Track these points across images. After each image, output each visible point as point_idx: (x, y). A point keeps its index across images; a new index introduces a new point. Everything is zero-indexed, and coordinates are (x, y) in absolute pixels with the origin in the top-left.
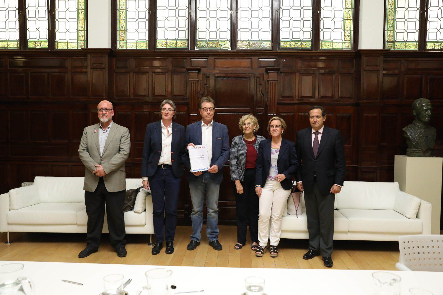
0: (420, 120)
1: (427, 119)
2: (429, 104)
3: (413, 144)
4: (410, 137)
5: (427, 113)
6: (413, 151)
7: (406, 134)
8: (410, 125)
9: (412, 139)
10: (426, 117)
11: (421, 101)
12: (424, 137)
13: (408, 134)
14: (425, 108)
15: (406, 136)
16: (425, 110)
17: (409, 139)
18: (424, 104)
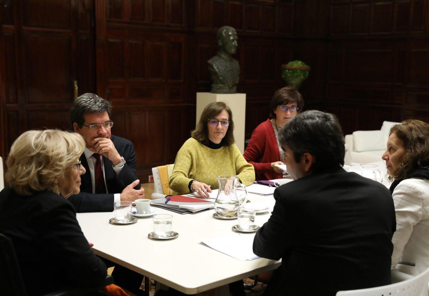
0: (226, 52)
1: (233, 51)
2: (235, 33)
3: (220, 79)
4: (217, 71)
5: (233, 43)
6: (220, 86)
7: (213, 67)
8: (216, 58)
9: (218, 73)
10: (233, 48)
11: (227, 30)
12: (231, 71)
13: (215, 68)
14: (231, 38)
15: (212, 69)
16: (232, 40)
17: (216, 73)
18: (230, 33)
